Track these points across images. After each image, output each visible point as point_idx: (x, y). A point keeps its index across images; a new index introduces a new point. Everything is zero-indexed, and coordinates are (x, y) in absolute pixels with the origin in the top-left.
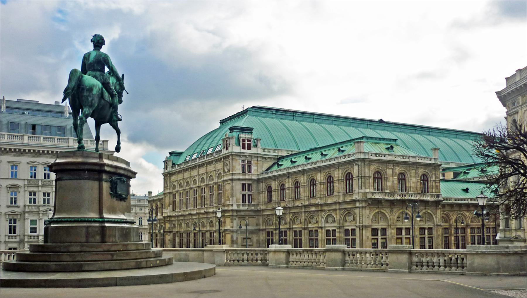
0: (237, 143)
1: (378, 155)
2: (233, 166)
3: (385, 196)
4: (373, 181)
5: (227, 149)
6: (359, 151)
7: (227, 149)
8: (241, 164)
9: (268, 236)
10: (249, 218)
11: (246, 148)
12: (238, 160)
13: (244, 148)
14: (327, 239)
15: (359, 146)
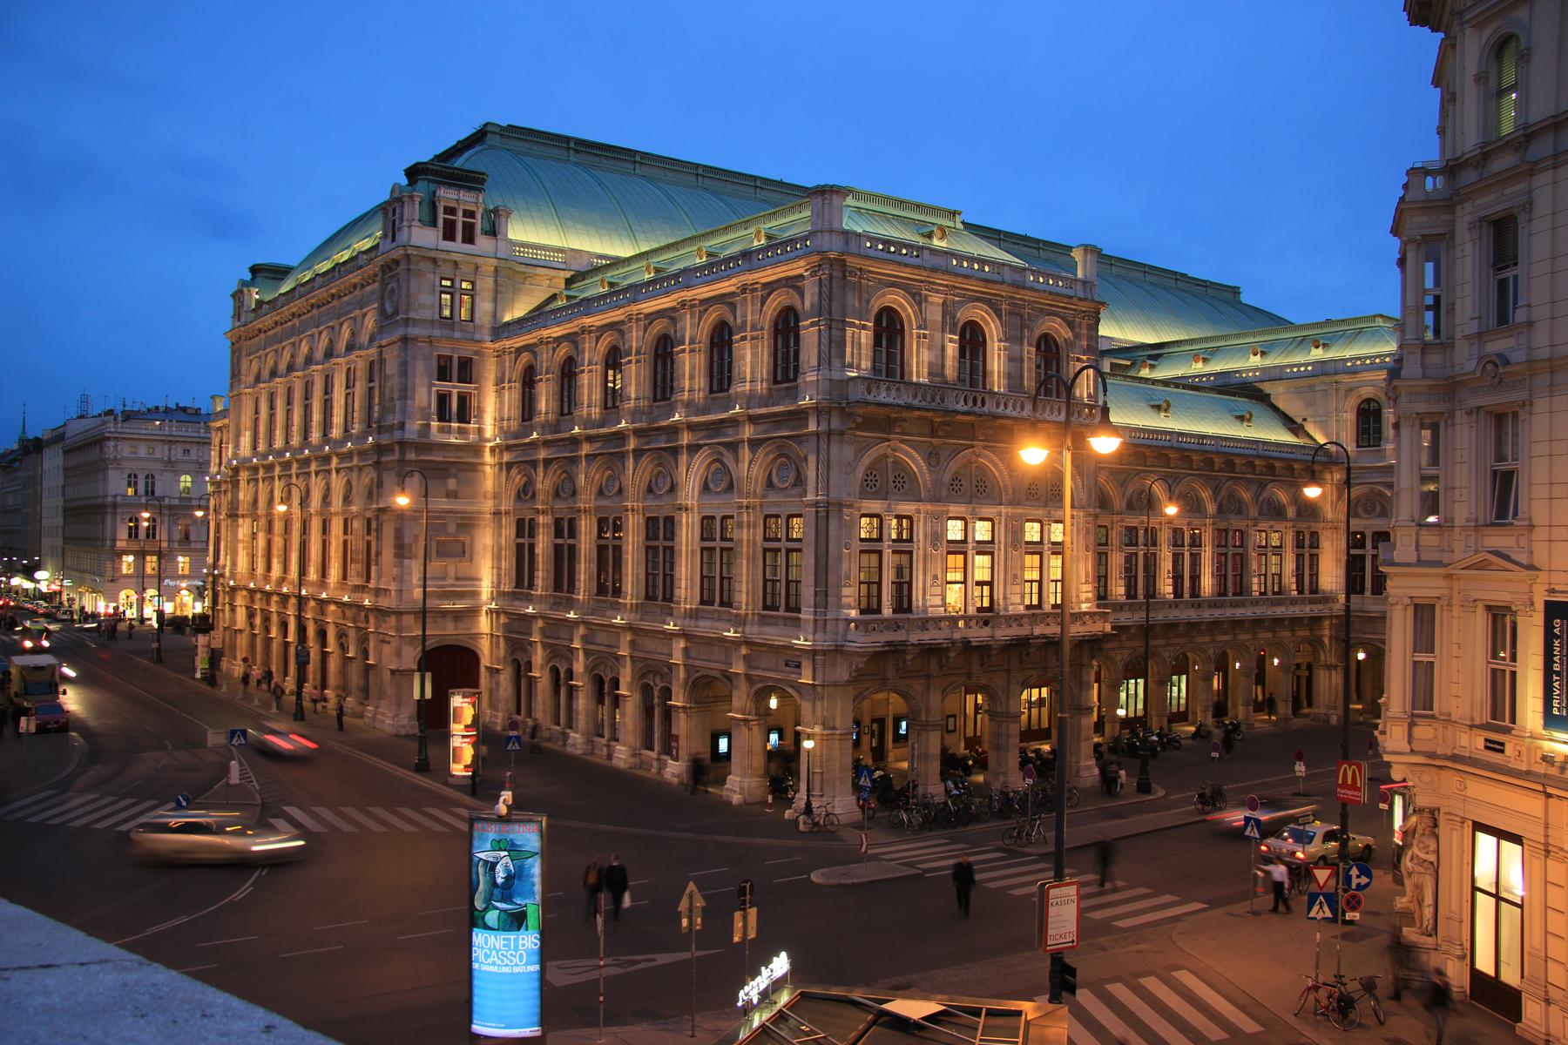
0: (426, 219)
1: (892, 249)
2: (408, 296)
3: (915, 396)
4: (871, 342)
5: (394, 240)
6: (827, 226)
7: (394, 240)
8: (438, 289)
9: (519, 534)
10: (458, 470)
11: (459, 236)
12: (430, 276)
13: (449, 235)
14: (703, 549)
15: (826, 206)
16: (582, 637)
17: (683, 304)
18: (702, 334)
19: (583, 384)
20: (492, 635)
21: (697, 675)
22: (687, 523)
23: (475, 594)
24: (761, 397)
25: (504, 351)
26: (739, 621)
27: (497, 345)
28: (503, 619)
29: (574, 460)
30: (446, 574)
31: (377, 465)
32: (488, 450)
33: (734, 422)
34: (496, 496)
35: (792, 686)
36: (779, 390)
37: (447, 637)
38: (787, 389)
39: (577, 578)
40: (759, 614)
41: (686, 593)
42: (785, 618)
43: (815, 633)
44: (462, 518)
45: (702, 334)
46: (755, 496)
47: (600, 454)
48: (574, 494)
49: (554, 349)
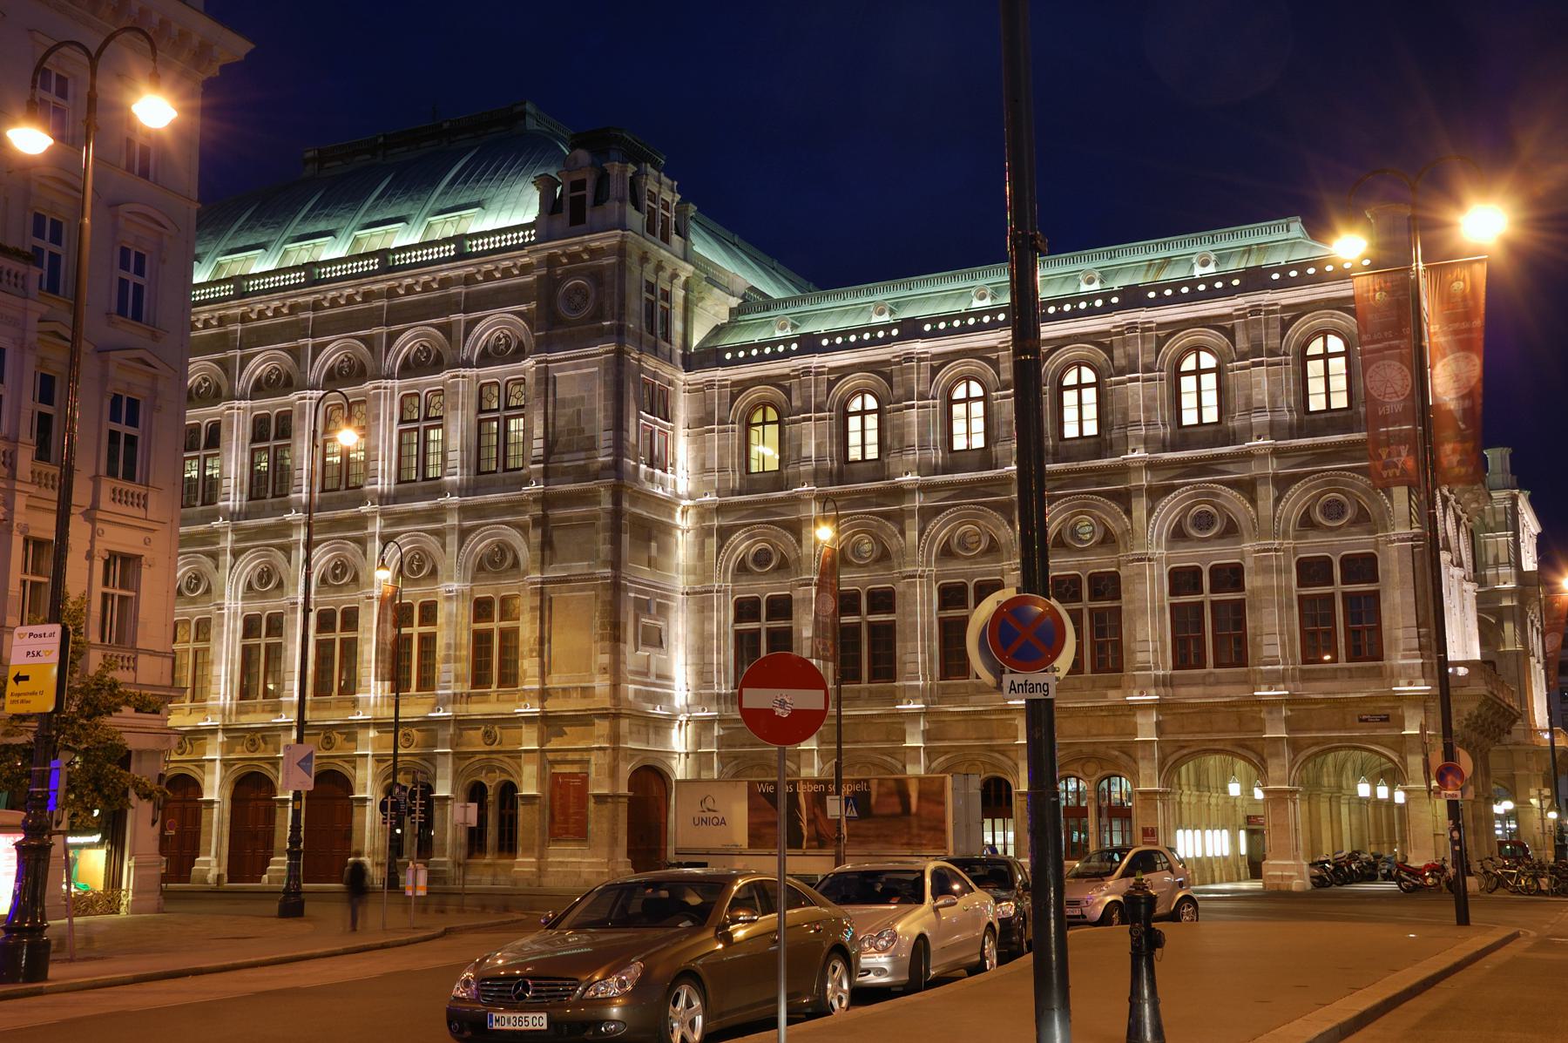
13: (651, 229)
16: (923, 731)
17: (1132, 327)
18: (1163, 362)
19: (910, 424)
20: (687, 755)
21: (1185, 752)
22: (1152, 576)
23: (670, 698)
24: (1291, 426)
25: (710, 384)
26: (1274, 680)
27: (689, 378)
28: (717, 730)
29: (899, 518)
30: (648, 668)
31: (542, 522)
32: (679, 510)
33: (1248, 456)
34: (701, 568)
35: (1377, 743)
36: (1314, 420)
37: (650, 755)
38: (1326, 418)
39: (909, 658)
40: (1301, 670)
41: (1156, 657)
42: (1349, 670)
43: (1424, 677)
44: (663, 596)
45: (1163, 362)
46: (1286, 535)
47: (954, 505)
48: (883, 556)
49: (831, 384)
